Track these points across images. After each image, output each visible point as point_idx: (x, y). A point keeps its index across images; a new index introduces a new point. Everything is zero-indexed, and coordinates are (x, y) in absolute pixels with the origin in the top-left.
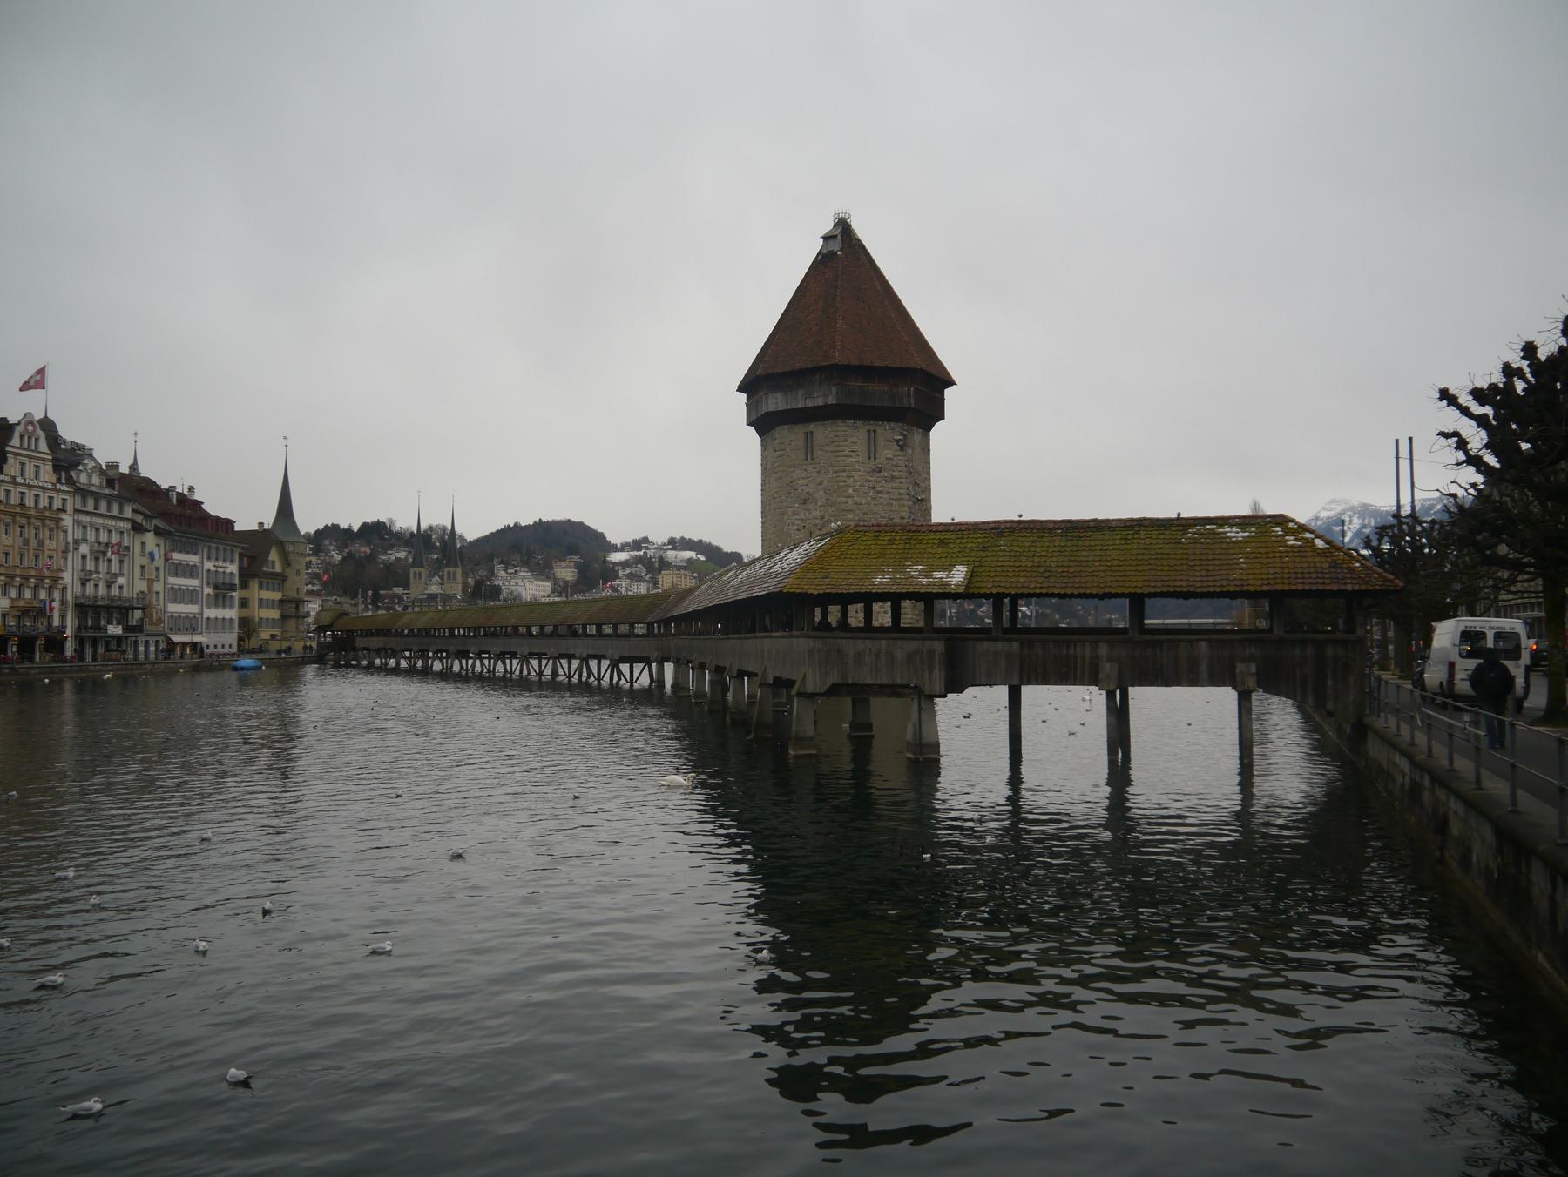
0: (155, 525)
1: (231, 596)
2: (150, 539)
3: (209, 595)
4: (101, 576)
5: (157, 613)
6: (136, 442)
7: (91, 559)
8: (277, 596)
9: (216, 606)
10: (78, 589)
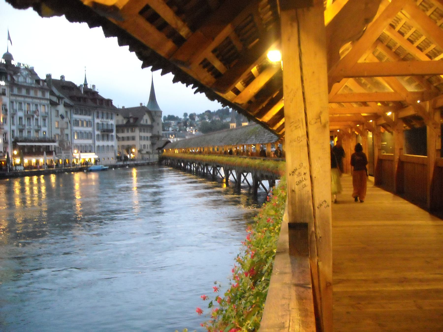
0: (64, 101)
1: (112, 136)
2: (61, 109)
3: (98, 135)
4: (32, 127)
5: (67, 144)
6: (85, 70)
7: (25, 119)
8: (149, 135)
9: (103, 140)
10: (17, 134)
